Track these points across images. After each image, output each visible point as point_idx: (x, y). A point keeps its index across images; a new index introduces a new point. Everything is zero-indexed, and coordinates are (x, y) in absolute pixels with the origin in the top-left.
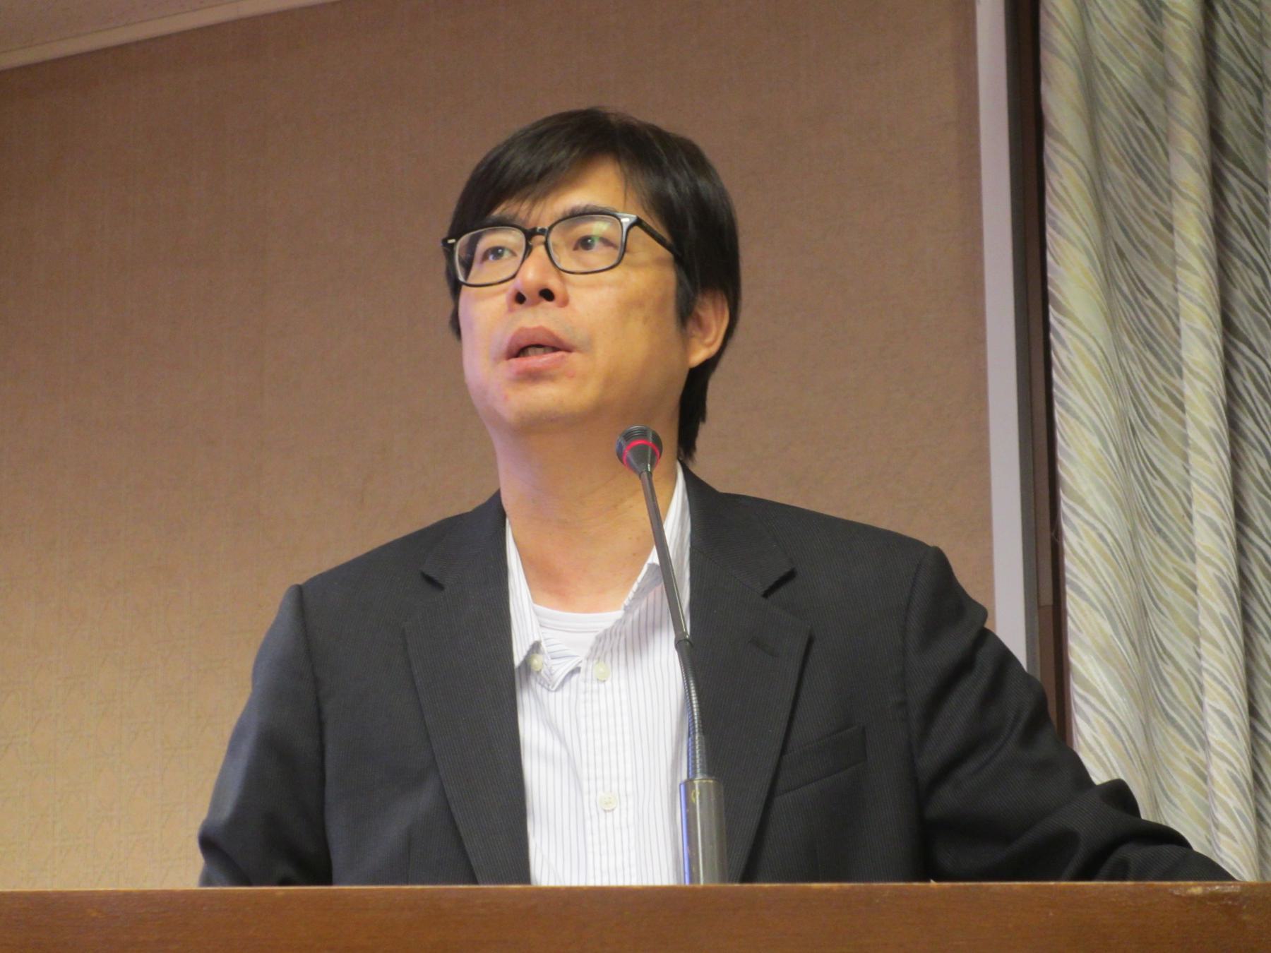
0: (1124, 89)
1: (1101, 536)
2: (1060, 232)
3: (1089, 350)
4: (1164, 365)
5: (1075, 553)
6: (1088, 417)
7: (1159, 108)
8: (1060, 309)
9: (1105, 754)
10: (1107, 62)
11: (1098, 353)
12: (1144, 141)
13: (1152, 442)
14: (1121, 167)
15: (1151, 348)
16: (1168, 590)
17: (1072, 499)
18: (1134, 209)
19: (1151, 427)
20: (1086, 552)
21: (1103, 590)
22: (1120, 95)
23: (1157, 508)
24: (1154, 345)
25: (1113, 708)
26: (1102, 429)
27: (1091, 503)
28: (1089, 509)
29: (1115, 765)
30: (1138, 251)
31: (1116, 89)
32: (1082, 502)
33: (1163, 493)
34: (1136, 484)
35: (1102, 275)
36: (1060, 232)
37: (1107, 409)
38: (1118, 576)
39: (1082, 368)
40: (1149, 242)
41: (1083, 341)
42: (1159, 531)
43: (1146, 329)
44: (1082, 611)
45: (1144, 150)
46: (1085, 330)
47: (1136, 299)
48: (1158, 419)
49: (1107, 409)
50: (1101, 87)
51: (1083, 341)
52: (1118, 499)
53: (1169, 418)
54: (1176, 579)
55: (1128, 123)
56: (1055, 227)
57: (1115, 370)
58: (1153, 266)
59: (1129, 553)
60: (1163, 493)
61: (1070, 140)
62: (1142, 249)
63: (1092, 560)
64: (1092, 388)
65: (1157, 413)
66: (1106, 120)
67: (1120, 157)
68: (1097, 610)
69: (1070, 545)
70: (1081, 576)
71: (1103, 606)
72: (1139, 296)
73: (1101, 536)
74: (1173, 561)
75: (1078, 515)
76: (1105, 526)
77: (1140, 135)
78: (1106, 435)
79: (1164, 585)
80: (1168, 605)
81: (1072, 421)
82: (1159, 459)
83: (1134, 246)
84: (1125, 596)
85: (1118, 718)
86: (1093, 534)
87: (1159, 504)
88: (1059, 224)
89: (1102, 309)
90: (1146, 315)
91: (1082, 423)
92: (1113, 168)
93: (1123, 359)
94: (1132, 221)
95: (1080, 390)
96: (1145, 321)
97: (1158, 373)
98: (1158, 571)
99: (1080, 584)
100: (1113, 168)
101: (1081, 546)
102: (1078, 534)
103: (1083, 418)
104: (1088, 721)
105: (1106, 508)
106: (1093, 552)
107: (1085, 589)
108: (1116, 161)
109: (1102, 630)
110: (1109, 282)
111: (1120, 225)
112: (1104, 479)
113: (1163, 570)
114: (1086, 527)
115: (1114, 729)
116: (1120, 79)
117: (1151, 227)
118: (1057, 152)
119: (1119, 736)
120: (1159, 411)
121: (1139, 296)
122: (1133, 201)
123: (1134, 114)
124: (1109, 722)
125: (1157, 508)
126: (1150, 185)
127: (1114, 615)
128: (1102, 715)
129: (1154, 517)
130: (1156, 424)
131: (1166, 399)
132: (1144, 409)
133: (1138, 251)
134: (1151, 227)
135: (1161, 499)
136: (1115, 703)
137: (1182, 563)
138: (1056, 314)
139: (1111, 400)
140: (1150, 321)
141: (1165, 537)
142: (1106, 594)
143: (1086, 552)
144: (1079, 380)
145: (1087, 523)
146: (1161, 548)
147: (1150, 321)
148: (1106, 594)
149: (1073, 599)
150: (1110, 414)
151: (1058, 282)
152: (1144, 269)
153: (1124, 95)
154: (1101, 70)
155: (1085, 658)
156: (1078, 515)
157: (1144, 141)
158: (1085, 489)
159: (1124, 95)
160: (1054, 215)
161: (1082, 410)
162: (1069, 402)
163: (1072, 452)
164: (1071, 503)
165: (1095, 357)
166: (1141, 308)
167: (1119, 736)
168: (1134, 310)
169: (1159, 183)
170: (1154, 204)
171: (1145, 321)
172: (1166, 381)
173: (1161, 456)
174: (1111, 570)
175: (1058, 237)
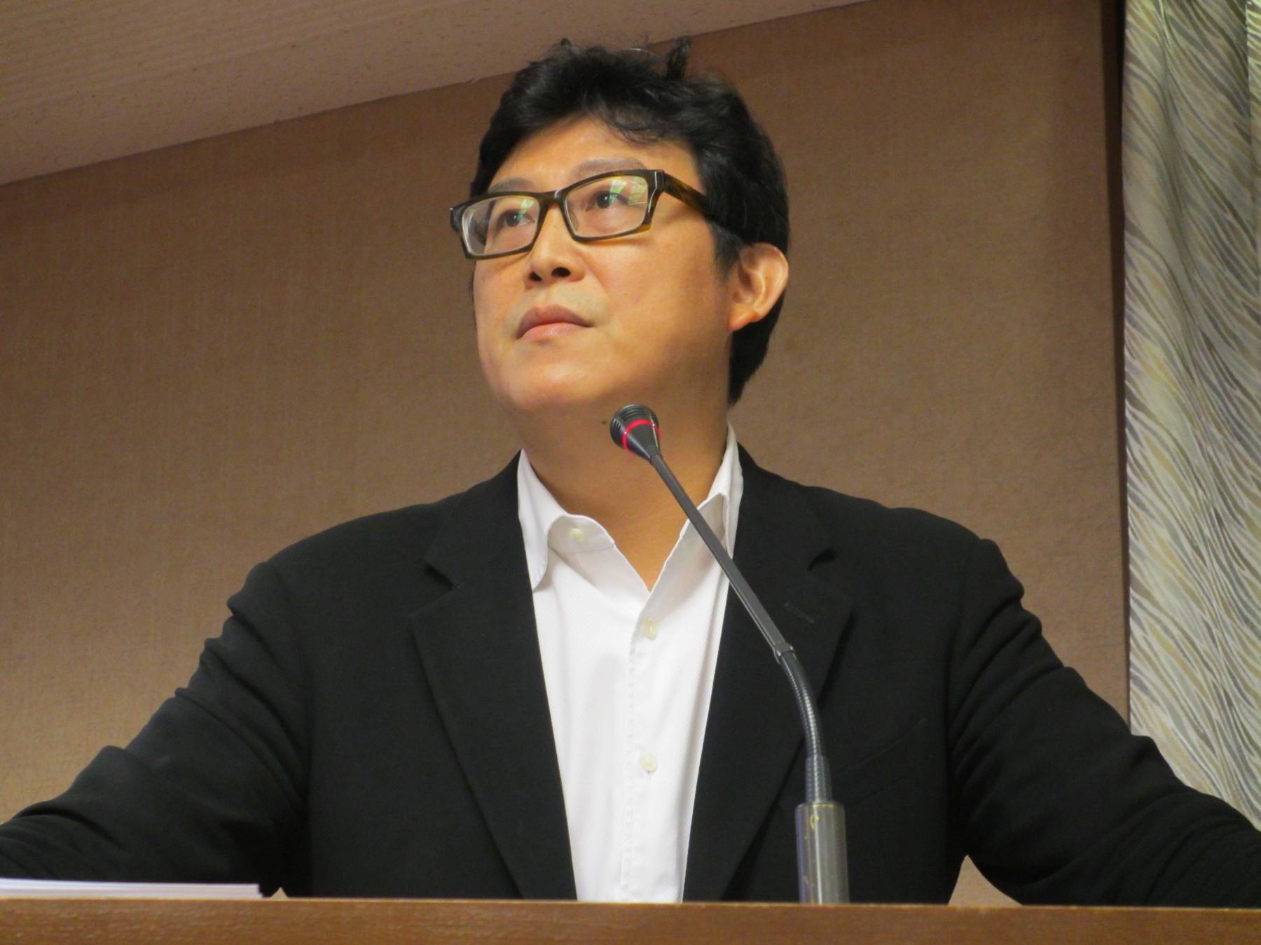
0: (1213, 183)
1: (1166, 629)
2: (1135, 326)
5: (1138, 646)
6: (1158, 510)
7: (1248, 202)
8: (1136, 403)
10: (1195, 156)
12: (1231, 233)
14: (1209, 258)
15: (1240, 439)
17: (1136, 591)
18: (1223, 301)
19: (1239, 517)
20: (1150, 645)
22: (1207, 188)
23: (1245, 599)
24: (1244, 437)
27: (1157, 595)
28: (1155, 603)
31: (1204, 183)
32: (1147, 595)
33: (1251, 584)
35: (1181, 367)
37: (1180, 500)
40: (1237, 333)
42: (1247, 621)
44: (1143, 705)
45: (1232, 243)
46: (1157, 422)
47: (1225, 390)
48: (1246, 509)
49: (1180, 500)
50: (1190, 182)
51: (1155, 434)
55: (1216, 215)
58: (1240, 357)
60: (1251, 584)
63: (1156, 655)
66: (1192, 211)
67: (1205, 245)
68: (1158, 703)
71: (1164, 699)
72: (1227, 385)
73: (1166, 629)
75: (1144, 609)
76: (1172, 619)
77: (1227, 227)
84: (1193, 688)
86: (1158, 627)
87: (1247, 594)
88: (1135, 317)
89: (1179, 401)
90: (1234, 405)
91: (1152, 516)
94: (1220, 311)
95: (1151, 483)
96: (1234, 413)
97: (1247, 464)
98: (1245, 662)
99: (1143, 679)
100: (1201, 259)
102: (1143, 629)
103: (1152, 510)
106: (1157, 647)
108: (1202, 248)
109: (1162, 725)
110: (1189, 370)
113: (1251, 661)
114: (1151, 621)
116: (1208, 172)
117: (1241, 320)
118: (1133, 245)
120: (1246, 500)
121: (1227, 385)
122: (1221, 292)
123: (1222, 207)
126: (1238, 276)
127: (1177, 708)
133: (1226, 340)
134: (1241, 320)
140: (1238, 412)
143: (1150, 645)
145: (1151, 615)
146: (1248, 638)
148: (1168, 686)
150: (1183, 505)
151: (1132, 375)
152: (1233, 359)
153: (1212, 188)
154: (1189, 165)
156: (1144, 609)
157: (1231, 233)
158: (1151, 583)
159: (1212, 188)
160: (1131, 309)
161: (1151, 503)
165: (1168, 450)
168: (1223, 401)
169: (1247, 275)
170: (1244, 297)
171: (1234, 413)
173: (1248, 545)
174: (1176, 664)
175: (1134, 330)
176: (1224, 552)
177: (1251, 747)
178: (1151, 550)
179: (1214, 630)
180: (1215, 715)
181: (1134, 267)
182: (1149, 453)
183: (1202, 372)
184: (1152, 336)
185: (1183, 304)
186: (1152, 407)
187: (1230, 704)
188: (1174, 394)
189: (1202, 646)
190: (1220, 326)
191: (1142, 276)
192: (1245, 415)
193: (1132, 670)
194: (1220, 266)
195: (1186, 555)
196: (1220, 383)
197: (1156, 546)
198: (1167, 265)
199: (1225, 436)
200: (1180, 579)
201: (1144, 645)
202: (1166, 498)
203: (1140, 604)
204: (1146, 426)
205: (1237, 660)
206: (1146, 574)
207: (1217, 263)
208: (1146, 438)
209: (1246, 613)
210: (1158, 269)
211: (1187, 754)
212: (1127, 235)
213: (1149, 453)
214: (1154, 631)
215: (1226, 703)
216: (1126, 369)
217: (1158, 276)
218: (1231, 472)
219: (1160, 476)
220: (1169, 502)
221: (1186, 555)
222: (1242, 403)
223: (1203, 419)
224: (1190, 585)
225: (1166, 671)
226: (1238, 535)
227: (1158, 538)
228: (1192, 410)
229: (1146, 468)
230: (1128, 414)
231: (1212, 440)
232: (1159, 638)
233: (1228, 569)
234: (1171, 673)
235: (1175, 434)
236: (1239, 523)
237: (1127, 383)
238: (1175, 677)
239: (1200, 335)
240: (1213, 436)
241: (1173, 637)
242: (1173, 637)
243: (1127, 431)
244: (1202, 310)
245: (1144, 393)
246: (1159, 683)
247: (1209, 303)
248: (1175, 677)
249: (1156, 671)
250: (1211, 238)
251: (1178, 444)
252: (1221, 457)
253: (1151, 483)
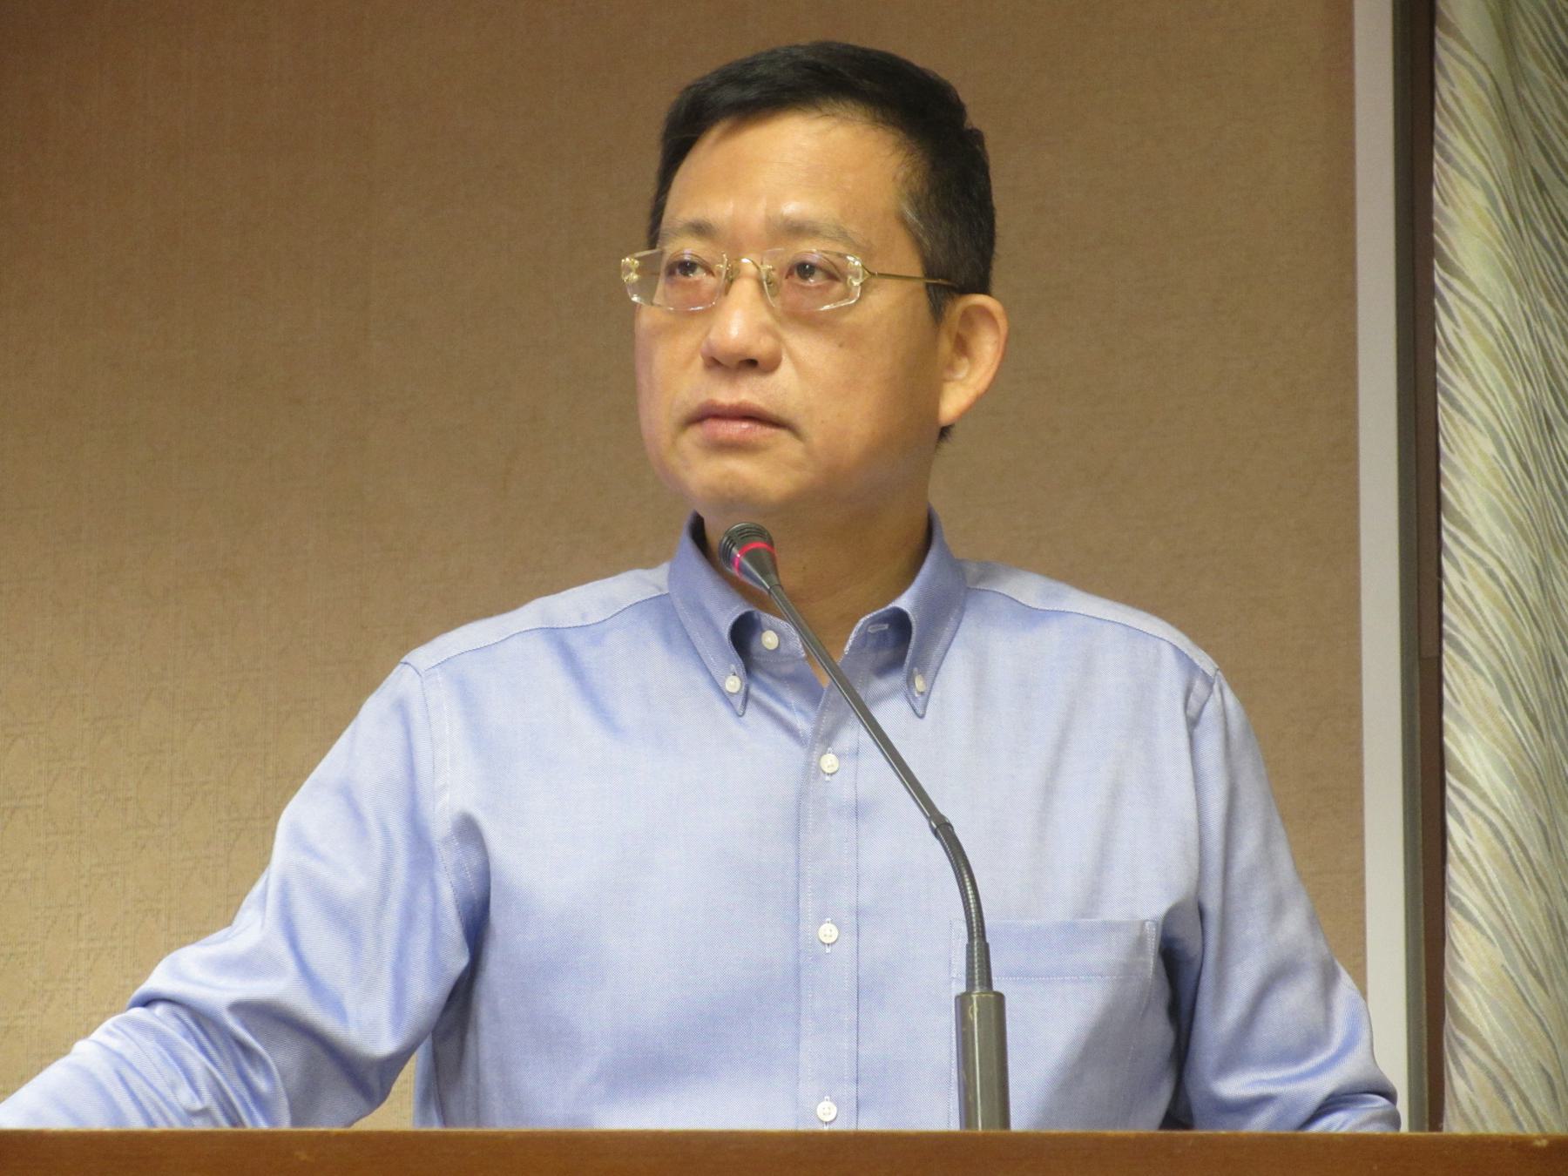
1: (1491, 574)
2: (1448, 159)
3: (1484, 321)
5: (1455, 596)
6: (1479, 413)
8: (1448, 267)
9: (1482, 867)
11: (1496, 324)
17: (1454, 523)
21: (1492, 647)
25: (1498, 805)
26: (1498, 429)
28: (1476, 538)
29: (1495, 881)
32: (1469, 530)
34: (1551, 499)
36: (1448, 159)
38: (1513, 624)
39: (1473, 346)
41: (1475, 310)
46: (1478, 294)
47: (1558, 245)
51: (1475, 310)
52: (1519, 526)
56: (1443, 153)
57: (1522, 346)
59: (1532, 595)
61: (1468, 37)
64: (1486, 375)
69: (1451, 588)
70: (1462, 627)
71: (1490, 667)
73: (1491, 574)
75: (1462, 545)
76: (1499, 560)
78: (1502, 436)
81: (1457, 417)
83: (1557, 173)
84: (1524, 653)
85: (1503, 817)
88: (1448, 147)
89: (1504, 264)
91: (1471, 421)
92: (1532, 65)
93: (1537, 327)
94: (1554, 137)
95: (1469, 376)
99: (1461, 639)
100: (1532, 65)
101: (1464, 587)
102: (1460, 572)
104: (1461, 822)
105: (1501, 536)
106: (1479, 596)
107: (1467, 646)
108: (1534, 52)
111: (1539, 143)
112: (1498, 495)
114: (1472, 562)
115: (1497, 833)
118: (1447, 48)
119: (1502, 841)
124: (1490, 824)
128: (1481, 814)
136: (1500, 798)
138: (1441, 272)
139: (1513, 389)
142: (1496, 651)
144: (1468, 363)
148: (1496, 651)
149: (1450, 658)
150: (1509, 407)
151: (1443, 227)
155: (1462, 738)
156: (1462, 545)
160: (1443, 137)
162: (1453, 390)
163: (1456, 459)
164: (1452, 528)
165: (1491, 330)
167: (1502, 841)
168: (1555, 259)
174: (1503, 619)
175: (1446, 166)
176: (1555, 469)
178: (1469, 464)
181: (1446, 76)
182: (1466, 335)
183: (1531, 222)
184: (1473, 177)
185: (1511, 133)
186: (1473, 275)
188: (1498, 255)
191: (1459, 91)
193: (1445, 626)
194: (1557, 76)
195: (1511, 469)
196: (1554, 238)
197: (1477, 461)
198: (1491, 76)
199: (1558, 310)
200: (1507, 507)
201: (1462, 594)
202: (1489, 395)
203: (1456, 539)
204: (1462, 298)
206: (1465, 498)
207: (1554, 72)
208: (1461, 313)
210: (1480, 82)
211: (1516, 741)
212: (1439, 32)
213: (1466, 335)
214: (1476, 576)
216: (1436, 218)
217: (1482, 94)
219: (1482, 368)
220: (1493, 403)
221: (1511, 469)
224: (1518, 513)
225: (1491, 629)
227: (1481, 452)
228: (1517, 273)
229: (1464, 356)
230: (1437, 280)
231: (1541, 315)
232: (1482, 585)
234: (1498, 631)
235: (1500, 310)
237: (1436, 236)
238: (1503, 638)
240: (1543, 309)
241: (1500, 585)
242: (1500, 585)
243: (1436, 303)
244: (1532, 141)
245: (1460, 253)
246: (1482, 645)
247: (1539, 126)
248: (1503, 638)
249: (1479, 629)
250: (1545, 36)
251: (1503, 324)
253: (1469, 376)
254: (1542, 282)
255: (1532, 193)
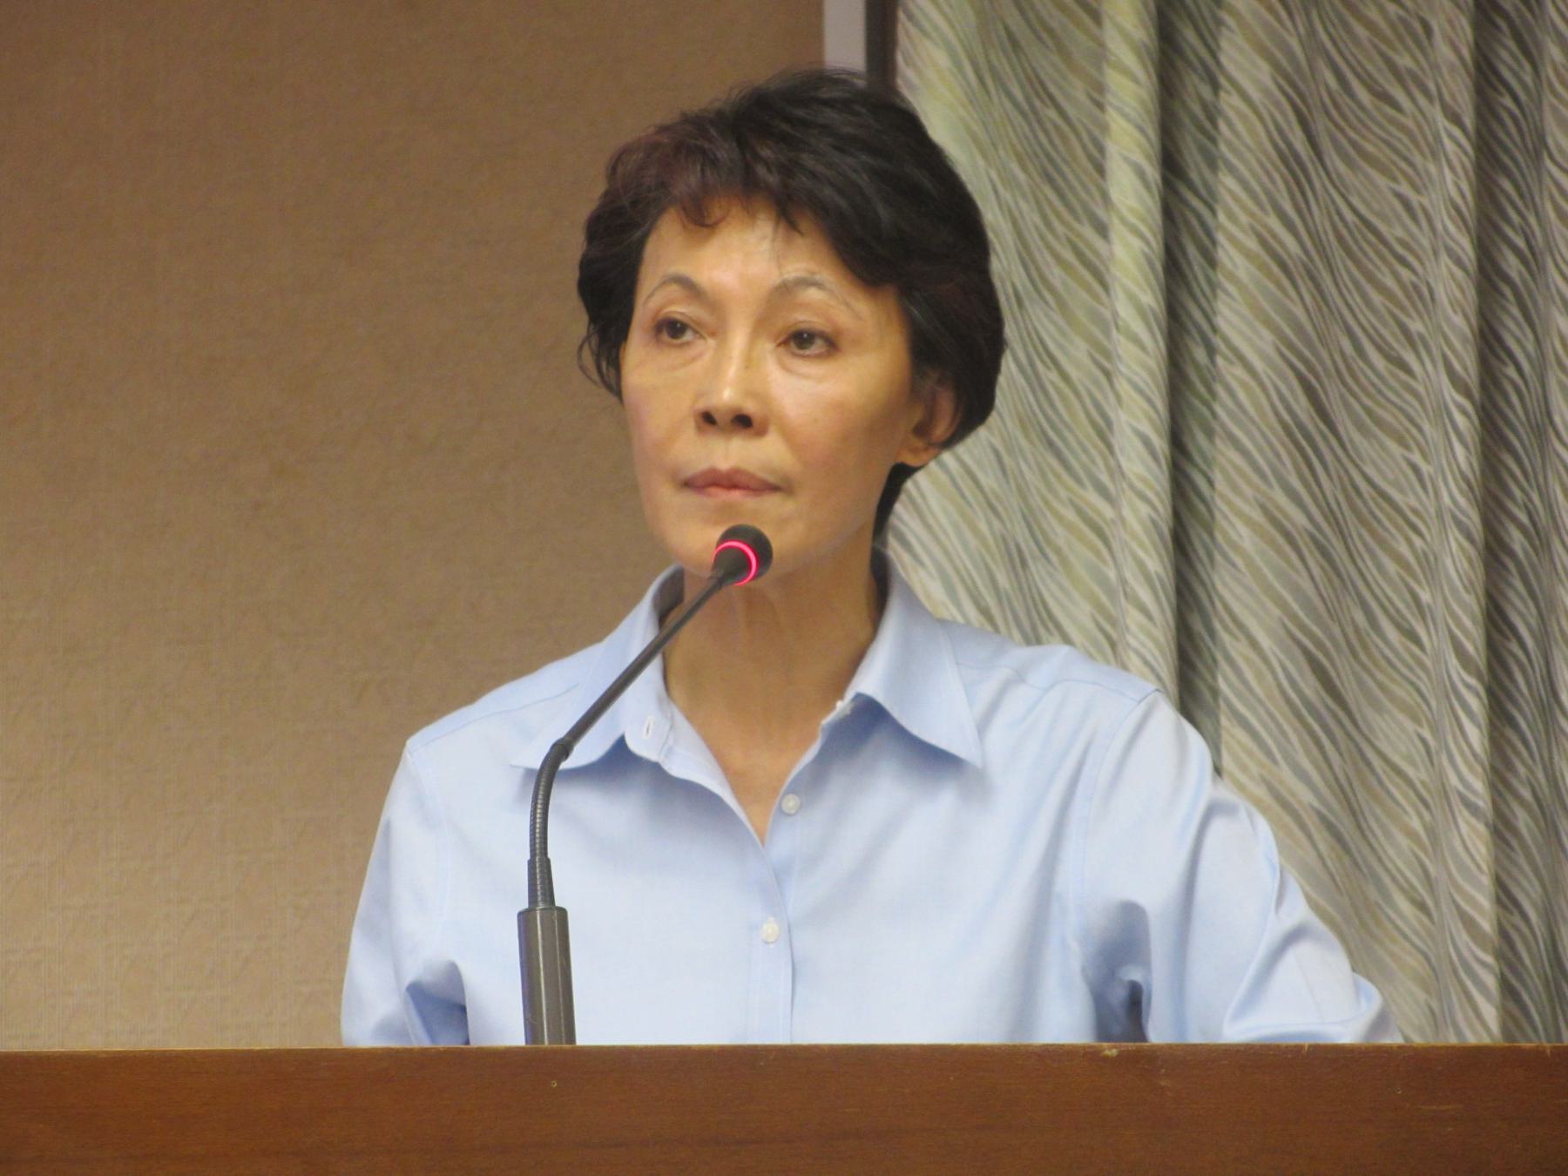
4: (1068, 205)
13: (1047, 315)
16: (1060, 530)
23: (1050, 412)
24: (1055, 175)
30: (1039, 38)
33: (1056, 388)
40: (1054, 24)
42: (1051, 444)
43: (1048, 155)
48: (1057, 283)
53: (1071, 282)
54: (1070, 515)
58: (1056, 58)
60: (1056, 388)
62: (1045, 35)
65: (1056, 274)
72: (1038, 103)
74: (1067, 488)
79: (1054, 522)
80: (1058, 551)
82: (1055, 340)
83: (1034, 31)
87: (1052, 405)
93: (1006, 195)
96: (1045, 141)
97: (1059, 216)
98: (1047, 503)
113: (1055, 504)
121: (1038, 103)
125: (1050, 412)
129: (1042, 420)
130: (1052, 289)
131: (1068, 255)
132: (1038, 269)
133: (1039, 38)
135: (1059, 404)
137: (1081, 492)
140: (1051, 142)
141: (1058, 455)
146: (1053, 470)
147: (1051, 142)
152: (1046, 64)
166: (1040, 122)
168: (1030, 124)
171: (1045, 141)
172: (1071, 229)
173: (1057, 336)
176: (1025, 346)
177: (1050, 625)
179: (1006, 459)
180: (1003, 580)
187: (1024, 563)
189: (989, 480)
190: (1031, 15)
192: (1061, 148)
196: (1028, 99)
205: (1036, 501)
209: (1051, 434)
215: (1017, 562)
218: (1037, 228)
222: (1057, 127)
223: (1002, 152)
226: (1045, 321)
233: (1028, 369)
236: (1046, 303)
239: (1001, 27)
252: (1024, 206)
254: (1013, 146)
255: (1004, 52)
